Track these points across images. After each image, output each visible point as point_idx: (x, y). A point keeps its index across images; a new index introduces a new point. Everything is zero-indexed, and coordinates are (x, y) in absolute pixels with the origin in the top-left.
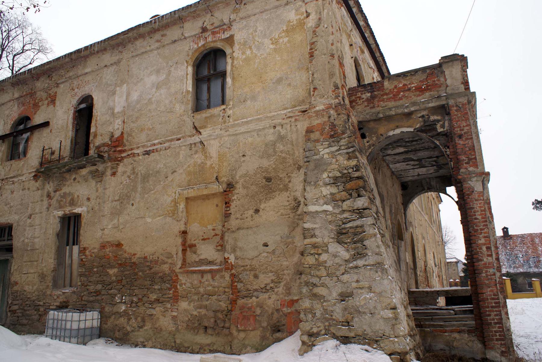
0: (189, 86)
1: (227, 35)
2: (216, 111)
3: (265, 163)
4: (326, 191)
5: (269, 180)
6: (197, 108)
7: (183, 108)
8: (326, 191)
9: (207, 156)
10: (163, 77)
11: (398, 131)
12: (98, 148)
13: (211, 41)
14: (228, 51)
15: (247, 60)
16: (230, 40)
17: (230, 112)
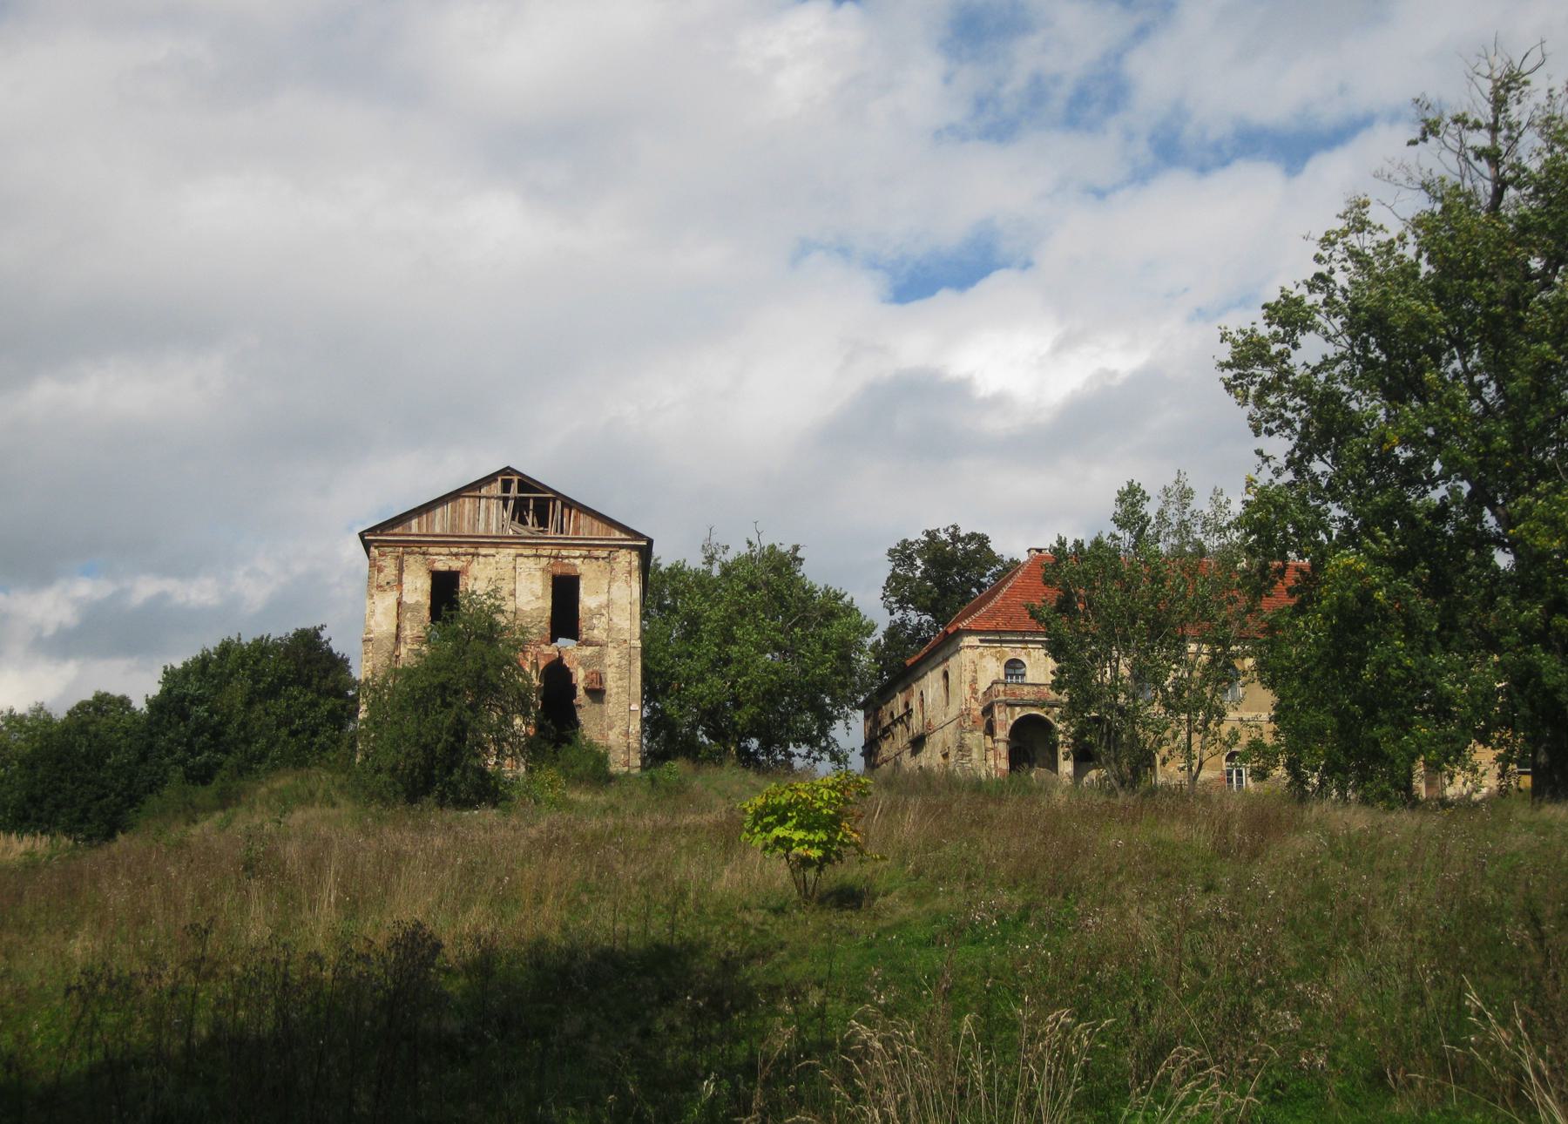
0: (942, 692)
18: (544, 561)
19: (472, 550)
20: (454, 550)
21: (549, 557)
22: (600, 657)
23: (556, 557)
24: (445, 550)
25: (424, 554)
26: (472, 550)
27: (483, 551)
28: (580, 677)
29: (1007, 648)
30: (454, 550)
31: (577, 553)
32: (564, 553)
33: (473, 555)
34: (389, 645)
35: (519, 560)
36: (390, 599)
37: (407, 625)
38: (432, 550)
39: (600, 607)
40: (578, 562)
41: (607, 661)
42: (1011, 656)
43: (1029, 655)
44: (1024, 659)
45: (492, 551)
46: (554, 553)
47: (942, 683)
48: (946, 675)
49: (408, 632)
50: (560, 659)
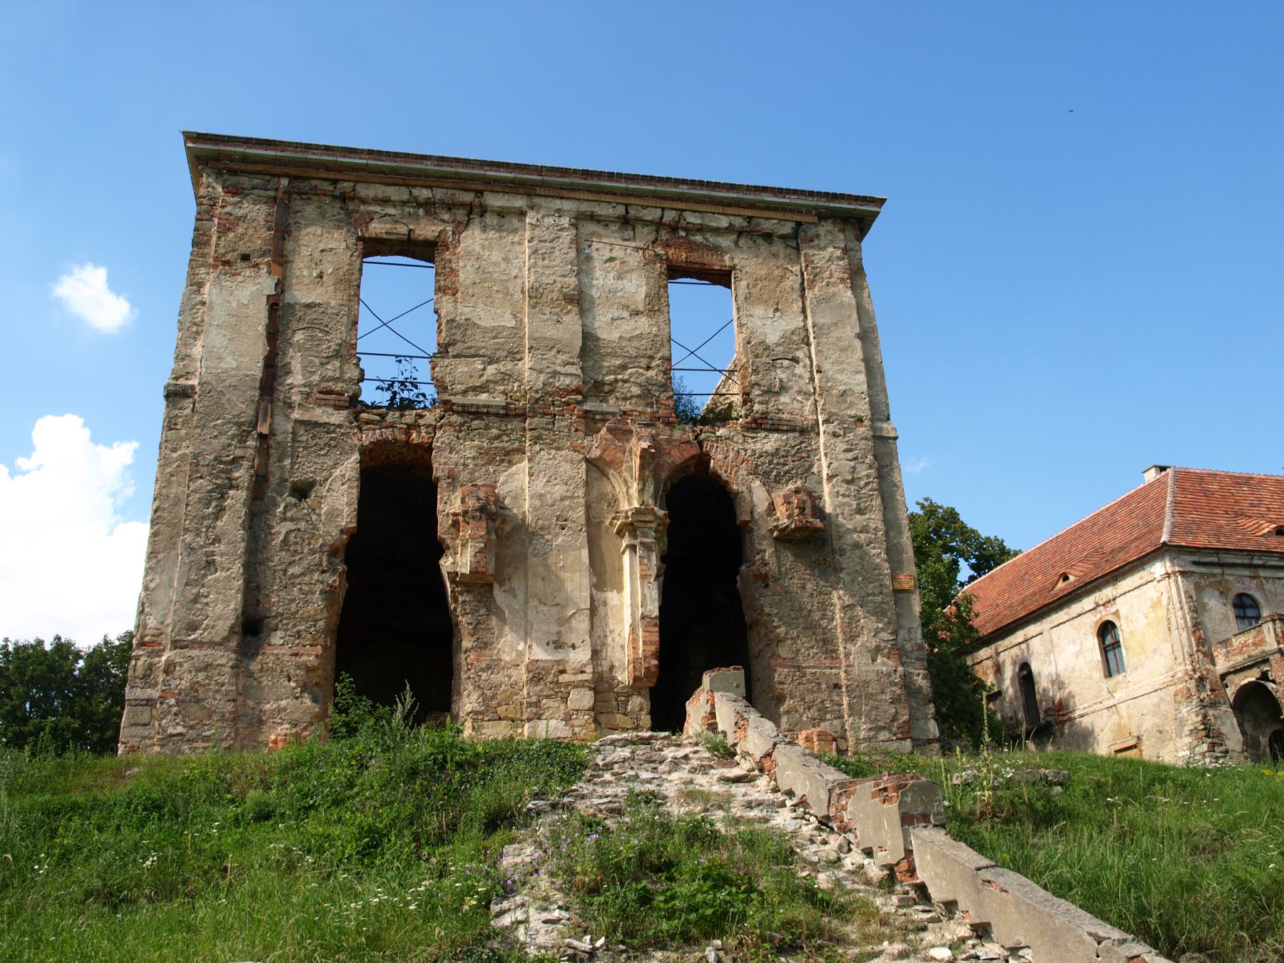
0: (1097, 655)
1: (1113, 610)
2: (1120, 677)
3: (1157, 720)
4: (1188, 740)
5: (1161, 732)
6: (1109, 674)
7: (1099, 673)
8: (1188, 740)
9: (1121, 717)
10: (1078, 648)
11: (1246, 681)
12: (1045, 712)
13: (1105, 614)
14: (1117, 624)
15: (1132, 632)
16: (1116, 613)
17: (1129, 678)
19: (468, 197)
20: (424, 194)
21: (658, 225)
23: (674, 228)
25: (344, 198)
26: (468, 197)
27: (495, 201)
28: (769, 506)
29: (1231, 576)
30: (424, 194)
31: (724, 222)
32: (692, 219)
33: (470, 209)
34: (242, 405)
35: (589, 227)
36: (253, 288)
37: (296, 362)
38: (365, 191)
39: (786, 339)
40: (725, 242)
41: (823, 466)
42: (1238, 588)
43: (1261, 588)
44: (1258, 595)
45: (519, 202)
46: (670, 216)
47: (1094, 641)
48: (1106, 629)
49: (296, 379)
50: (702, 459)
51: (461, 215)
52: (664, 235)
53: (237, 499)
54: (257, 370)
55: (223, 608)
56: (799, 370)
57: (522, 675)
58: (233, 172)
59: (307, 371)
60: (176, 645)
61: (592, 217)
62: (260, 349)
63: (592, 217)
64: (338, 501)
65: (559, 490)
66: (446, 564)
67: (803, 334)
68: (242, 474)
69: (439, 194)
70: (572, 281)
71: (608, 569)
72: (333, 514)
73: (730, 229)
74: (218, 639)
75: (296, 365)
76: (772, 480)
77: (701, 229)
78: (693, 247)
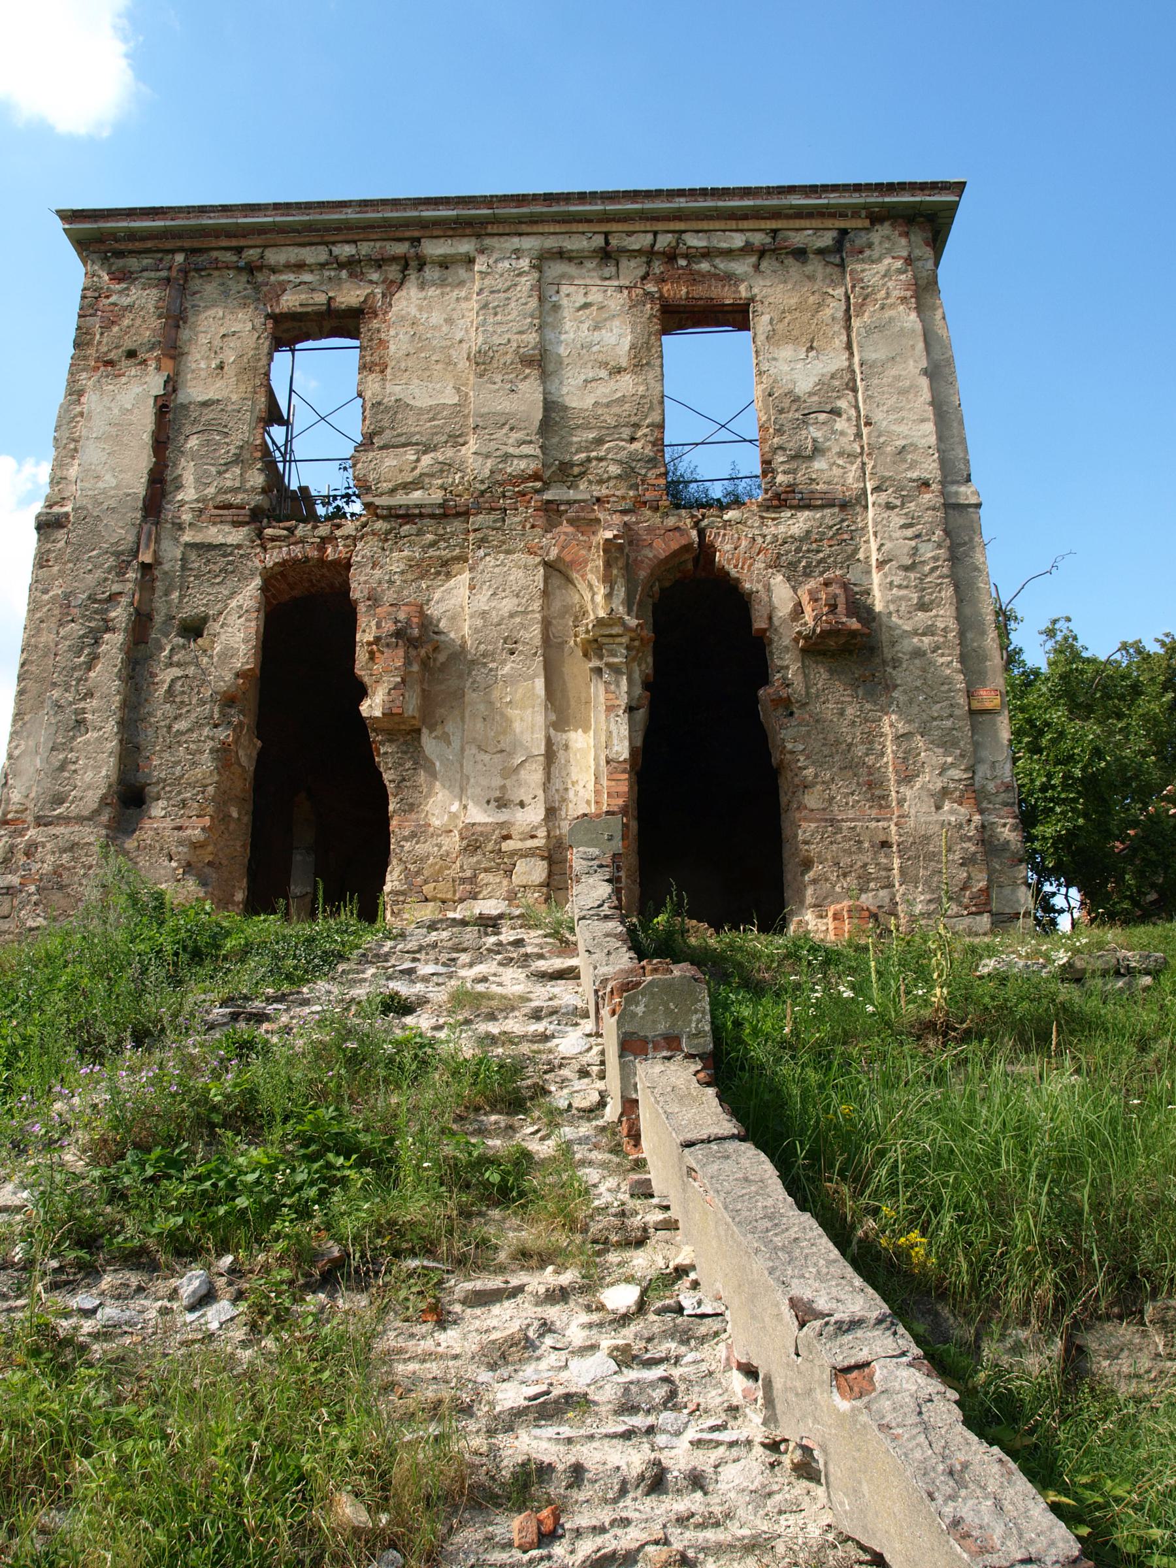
18: (631, 270)
19: (400, 249)
20: (347, 250)
21: (650, 254)
22: (846, 541)
23: (671, 257)
24: (314, 255)
25: (251, 269)
26: (400, 249)
27: (434, 248)
28: (785, 602)
30: (347, 250)
31: (738, 241)
32: (695, 241)
33: (404, 263)
34: (120, 530)
35: (556, 269)
36: (138, 391)
37: (188, 471)
38: (276, 257)
39: (824, 386)
40: (741, 267)
41: (871, 550)
45: (465, 246)
46: (664, 241)
49: (188, 494)
50: (705, 552)
51: (393, 271)
52: (658, 268)
53: (113, 643)
54: (139, 486)
55: (95, 774)
56: (840, 424)
57: (453, 843)
58: (119, 254)
59: (201, 483)
60: (40, 821)
61: (561, 255)
62: (143, 461)
63: (561, 255)
64: (235, 638)
65: (508, 605)
66: (365, 708)
67: (847, 377)
68: (119, 614)
69: (365, 248)
70: (532, 338)
71: (573, 703)
72: (228, 654)
73: (747, 249)
74: (86, 813)
75: (188, 478)
76: (795, 573)
77: (707, 254)
78: (695, 278)
